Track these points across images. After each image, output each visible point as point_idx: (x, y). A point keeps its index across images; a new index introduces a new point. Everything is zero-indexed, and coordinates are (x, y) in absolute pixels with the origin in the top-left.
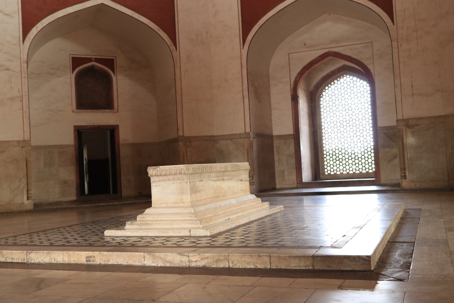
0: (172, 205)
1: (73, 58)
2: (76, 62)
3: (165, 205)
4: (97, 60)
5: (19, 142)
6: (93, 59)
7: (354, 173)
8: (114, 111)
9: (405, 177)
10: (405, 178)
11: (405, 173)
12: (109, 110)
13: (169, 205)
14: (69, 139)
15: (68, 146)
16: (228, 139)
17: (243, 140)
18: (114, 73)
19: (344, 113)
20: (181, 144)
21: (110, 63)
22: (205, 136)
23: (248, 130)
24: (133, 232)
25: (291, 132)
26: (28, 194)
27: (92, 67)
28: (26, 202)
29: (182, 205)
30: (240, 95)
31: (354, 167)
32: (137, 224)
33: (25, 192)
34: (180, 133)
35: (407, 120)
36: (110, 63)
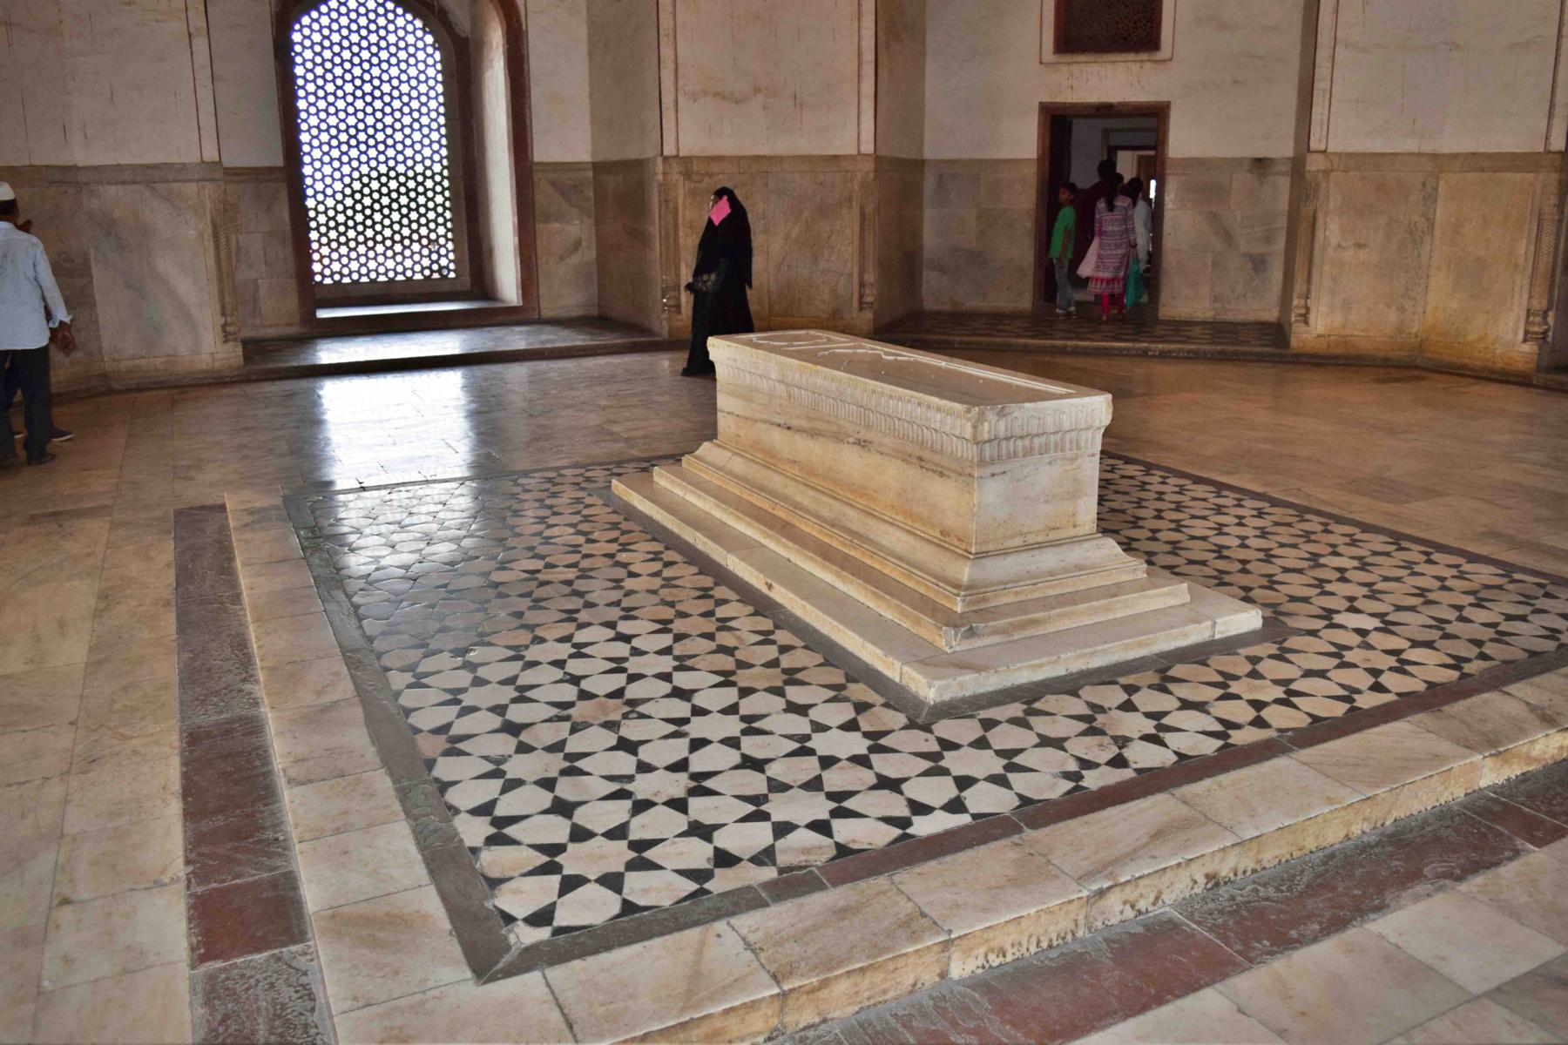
0: (1041, 539)
3: (1018, 541)
7: (392, 280)
10: (679, 312)
13: (1032, 539)
16: (134, 182)
17: (193, 187)
19: (359, 104)
23: (210, 154)
24: (1042, 666)
25: (279, 162)
29: (1072, 532)
30: (177, 26)
31: (390, 264)
32: (995, 632)
35: (686, 161)
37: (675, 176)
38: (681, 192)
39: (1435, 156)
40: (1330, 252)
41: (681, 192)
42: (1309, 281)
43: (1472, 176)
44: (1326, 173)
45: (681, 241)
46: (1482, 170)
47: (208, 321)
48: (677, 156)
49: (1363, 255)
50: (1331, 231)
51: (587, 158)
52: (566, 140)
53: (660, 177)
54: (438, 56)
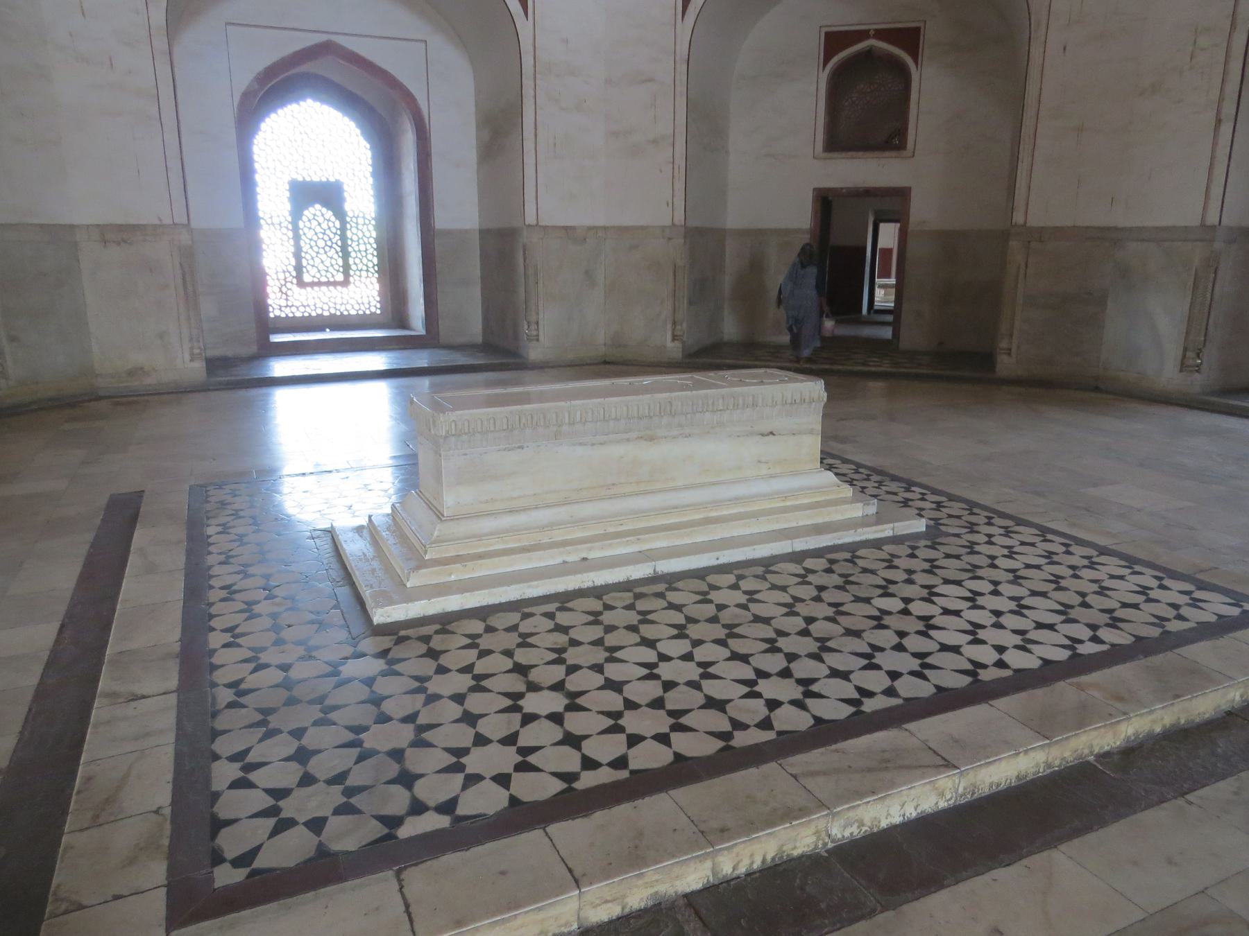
1: (827, 34)
2: (834, 41)
4: (881, 34)
5: (663, 228)
6: (872, 33)
8: (905, 153)
12: (893, 154)
14: (799, 217)
15: (796, 231)
18: (916, 63)
20: (1014, 244)
21: (909, 38)
22: (1087, 228)
23: (1213, 219)
26: (674, 330)
27: (869, 54)
28: (670, 344)
30: (1210, 116)
33: (669, 326)
34: (1018, 218)
36: (909, 38)
47: (1173, 351)
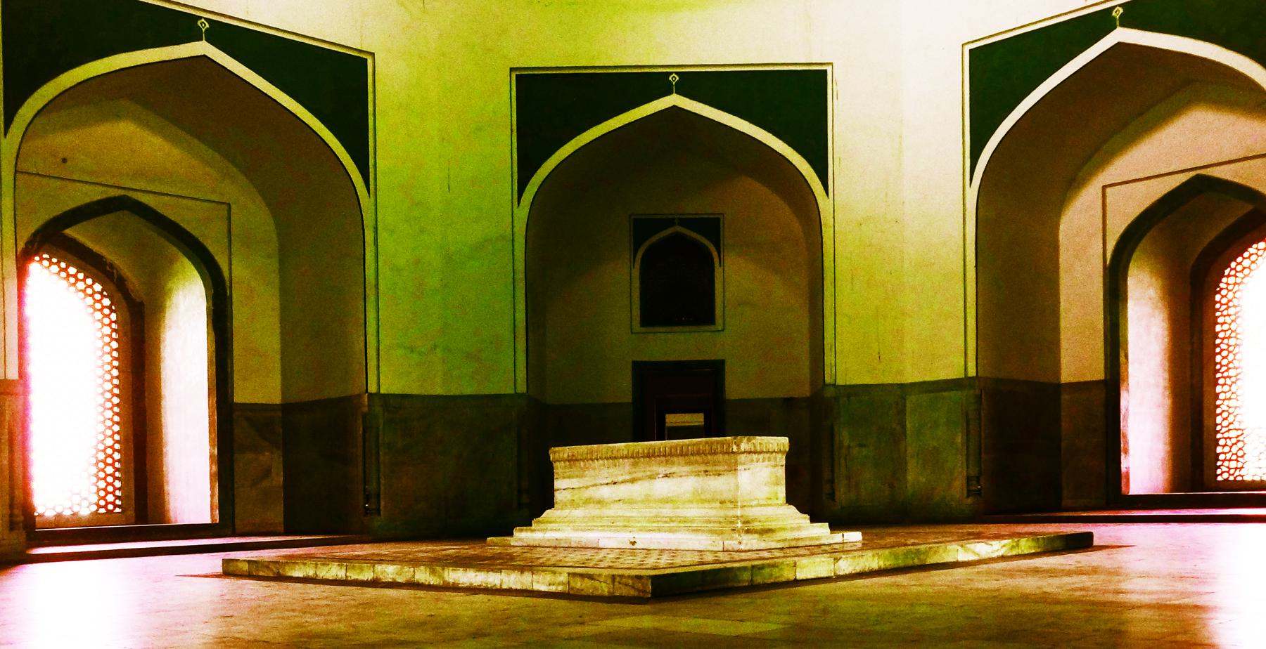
9: (378, 511)
11: (379, 503)
37: (378, 409)
38: (381, 421)
39: (902, 386)
40: (844, 451)
41: (381, 421)
42: (832, 471)
43: (925, 397)
44: (836, 399)
45: (382, 458)
46: (931, 392)
48: (378, 394)
49: (864, 451)
50: (844, 436)
51: (276, 399)
52: (260, 386)
53: (365, 409)
54: (114, 317)
